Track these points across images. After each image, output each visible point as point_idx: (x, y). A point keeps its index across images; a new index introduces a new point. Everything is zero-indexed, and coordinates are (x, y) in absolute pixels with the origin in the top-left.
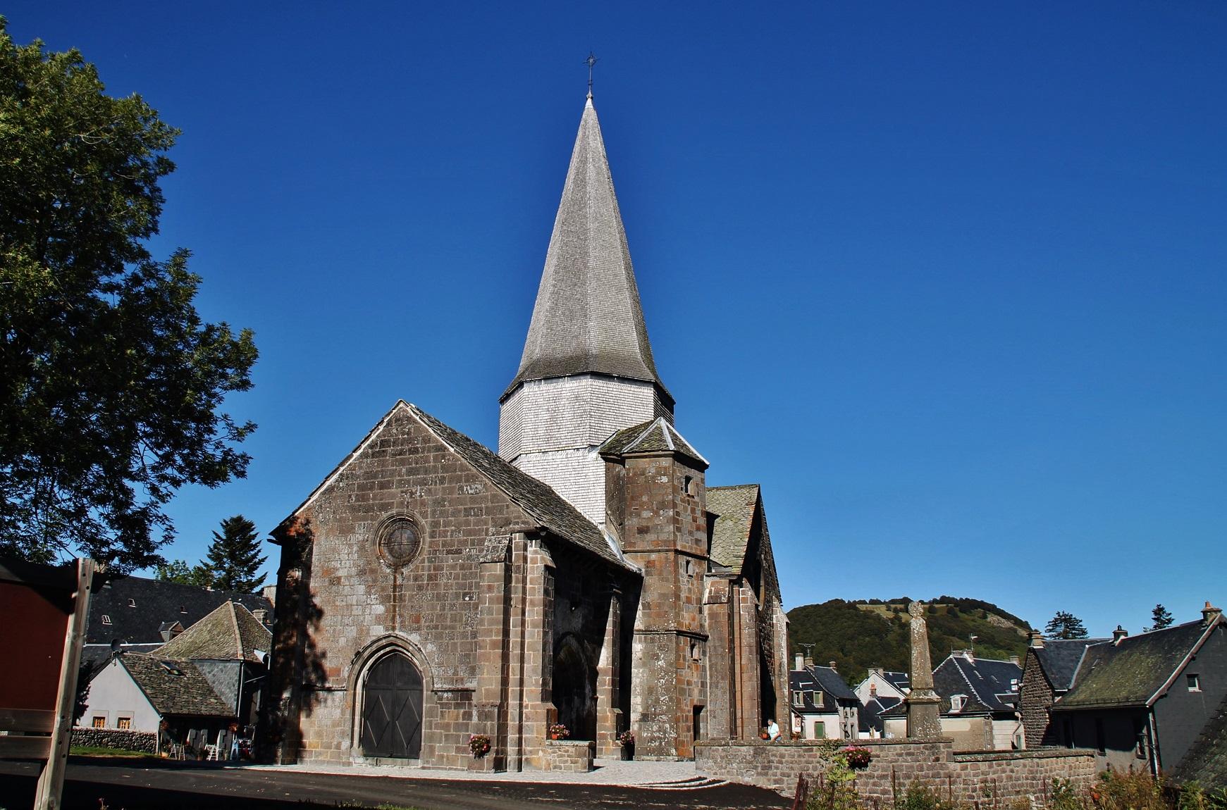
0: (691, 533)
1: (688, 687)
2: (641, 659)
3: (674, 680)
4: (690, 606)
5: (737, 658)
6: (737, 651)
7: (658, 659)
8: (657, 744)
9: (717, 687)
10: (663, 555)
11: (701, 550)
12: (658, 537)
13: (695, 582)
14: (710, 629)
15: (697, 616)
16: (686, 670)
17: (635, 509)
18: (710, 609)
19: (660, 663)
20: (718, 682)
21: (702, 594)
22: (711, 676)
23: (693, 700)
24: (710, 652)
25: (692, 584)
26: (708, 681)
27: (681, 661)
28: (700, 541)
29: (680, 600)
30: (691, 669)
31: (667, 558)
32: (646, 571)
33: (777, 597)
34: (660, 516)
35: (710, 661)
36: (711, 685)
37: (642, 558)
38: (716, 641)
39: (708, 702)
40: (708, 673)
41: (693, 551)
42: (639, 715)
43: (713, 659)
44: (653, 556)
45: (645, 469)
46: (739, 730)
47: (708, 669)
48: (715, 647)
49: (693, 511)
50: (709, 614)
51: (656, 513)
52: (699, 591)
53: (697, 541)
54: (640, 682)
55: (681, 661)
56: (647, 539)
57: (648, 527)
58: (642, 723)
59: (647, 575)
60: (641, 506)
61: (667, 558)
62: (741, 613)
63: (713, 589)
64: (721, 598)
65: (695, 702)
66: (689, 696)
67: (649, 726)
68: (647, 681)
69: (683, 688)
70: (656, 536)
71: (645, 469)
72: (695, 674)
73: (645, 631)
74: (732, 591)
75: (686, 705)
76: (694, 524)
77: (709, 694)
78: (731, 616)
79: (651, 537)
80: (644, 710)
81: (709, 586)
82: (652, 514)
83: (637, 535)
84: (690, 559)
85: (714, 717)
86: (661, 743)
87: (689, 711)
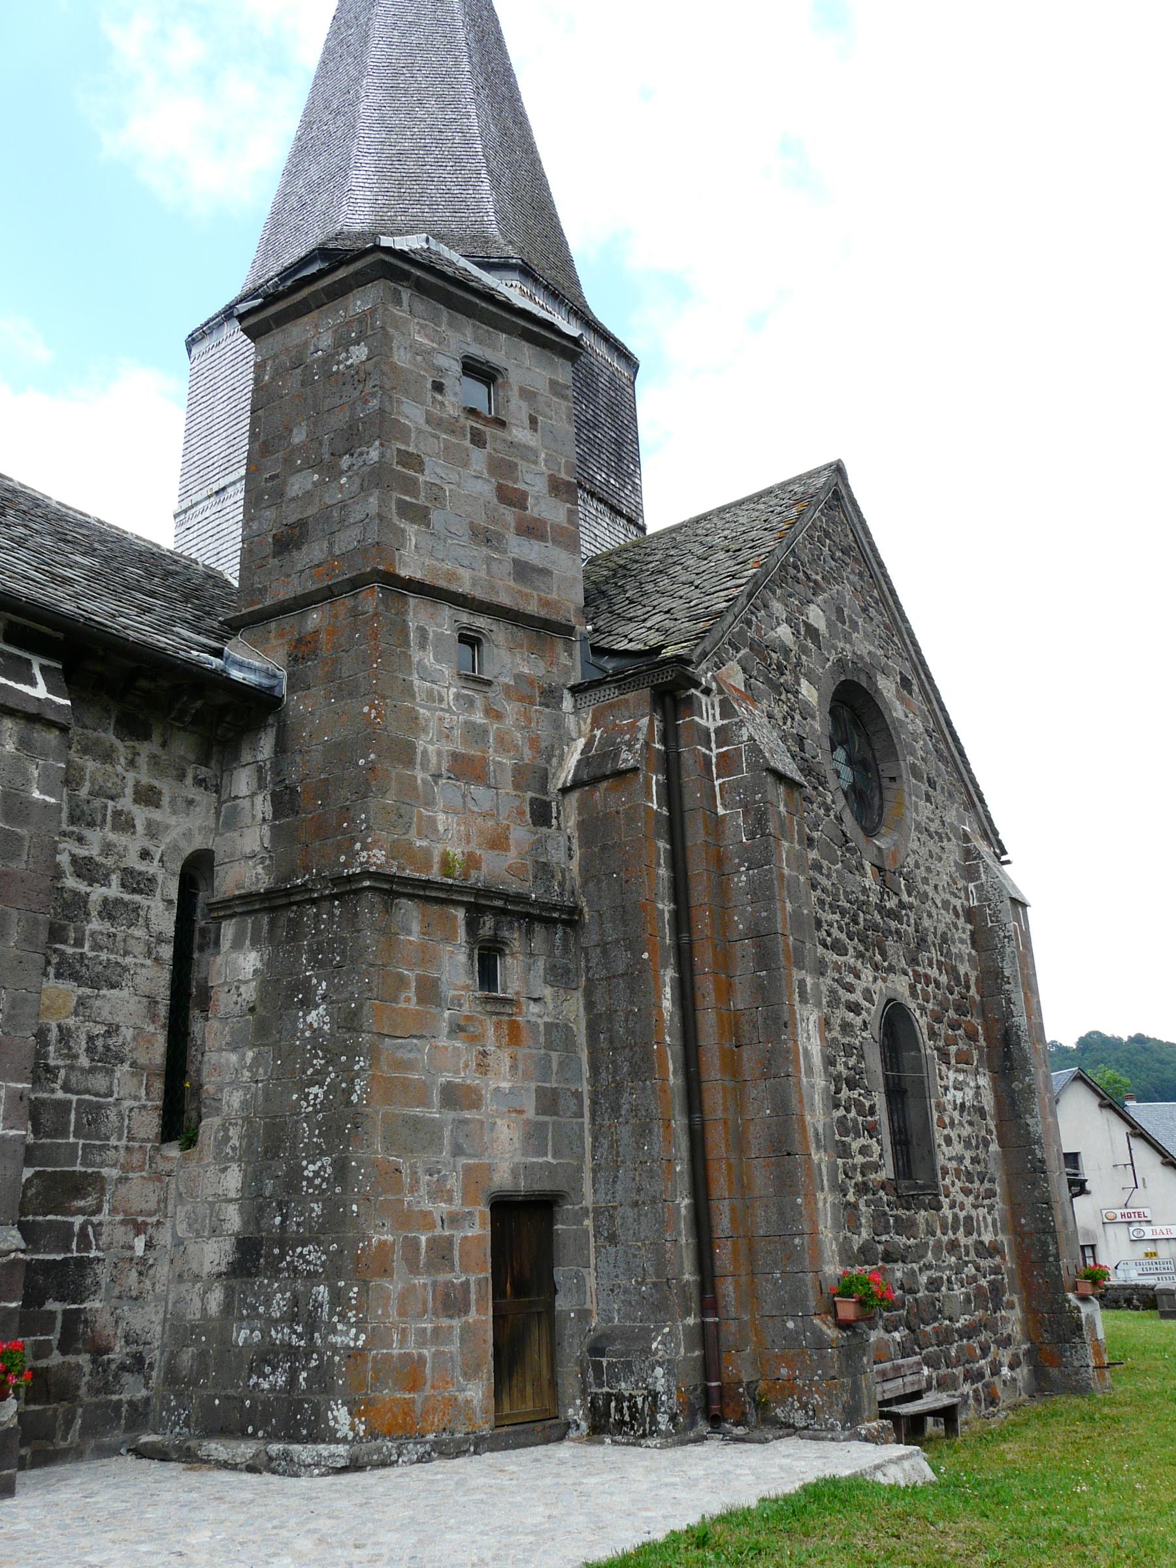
0: (485, 537)
1: (450, 1115)
2: (252, 1010)
3: (359, 1084)
4: (478, 791)
5: (706, 986)
6: (704, 959)
7: (308, 1004)
8: (281, 1380)
9: (615, 1110)
10: (345, 603)
11: (545, 603)
12: (331, 545)
13: (511, 709)
14: (585, 884)
15: (521, 834)
16: (443, 1041)
17: (272, 478)
18: (583, 806)
19: (312, 1017)
20: (619, 1088)
21: (552, 752)
22: (595, 1068)
23: (490, 1169)
24: (588, 969)
25: (493, 713)
26: (585, 1088)
27: (409, 1000)
28: (545, 572)
29: (411, 763)
30: (474, 1039)
31: (355, 613)
32: (290, 676)
33: (985, 836)
34: (342, 473)
35: (590, 1006)
36: (594, 1102)
37: (281, 634)
38: (608, 925)
39: (587, 1175)
40: (584, 1056)
41: (505, 600)
42: (228, 1245)
43: (597, 997)
44: (315, 618)
45: (306, 344)
46: (728, 1289)
47: (582, 1039)
48: (605, 952)
49: (501, 468)
50: (581, 825)
51: (331, 471)
52: (534, 742)
53: (523, 570)
54: (245, 1104)
55: (409, 1000)
56: (299, 567)
57: (302, 524)
58: (233, 1282)
59: (292, 688)
60: (288, 461)
61: (355, 613)
62: (721, 811)
63: (598, 733)
64: (617, 755)
65: (503, 1178)
66: (458, 1151)
67: (256, 1295)
68: (267, 1099)
69: (415, 1124)
70: (326, 544)
71: (306, 344)
72: (501, 1059)
73: (269, 894)
74: (670, 735)
75: (439, 1192)
76: (509, 515)
77: (588, 1140)
78: (675, 828)
79: (314, 552)
80: (245, 1223)
81: (586, 727)
82: (316, 477)
83: (273, 562)
84: (481, 622)
85: (612, 1239)
86: (292, 1380)
87: (454, 1220)
